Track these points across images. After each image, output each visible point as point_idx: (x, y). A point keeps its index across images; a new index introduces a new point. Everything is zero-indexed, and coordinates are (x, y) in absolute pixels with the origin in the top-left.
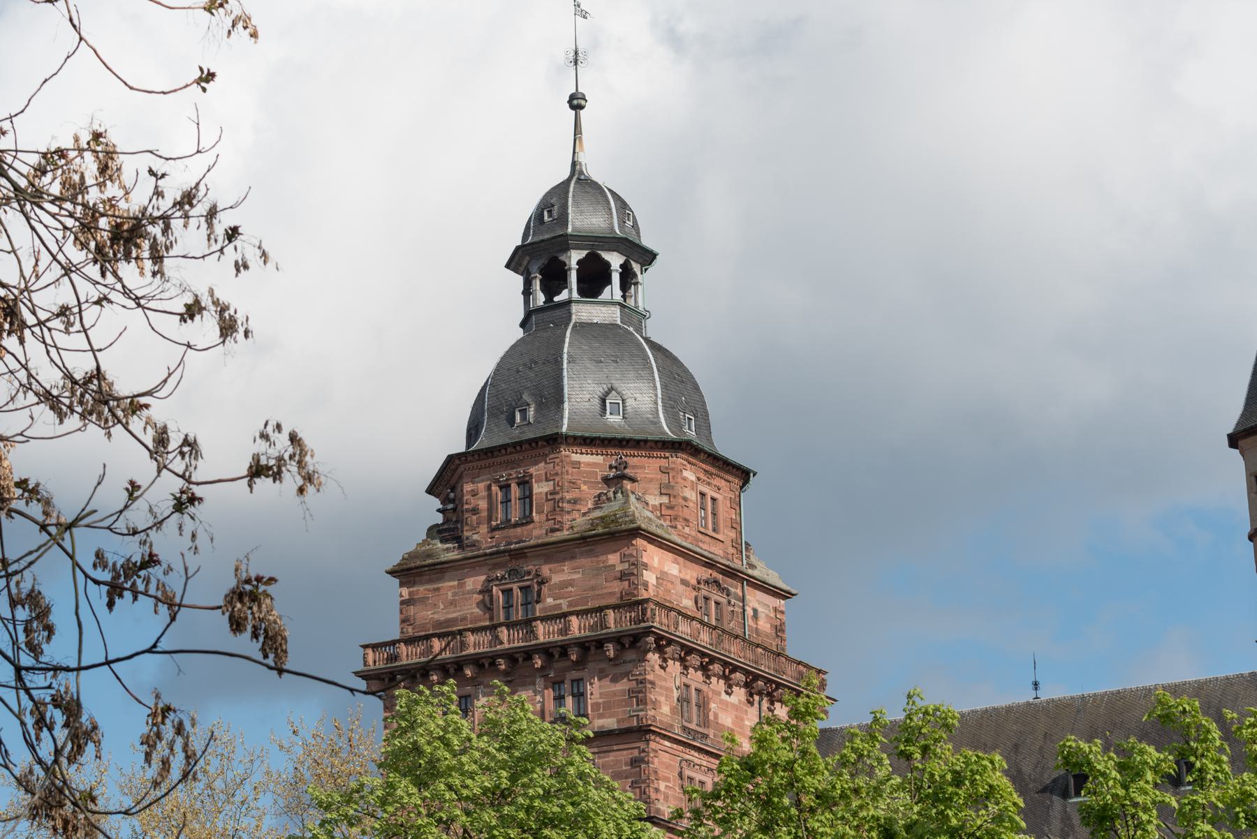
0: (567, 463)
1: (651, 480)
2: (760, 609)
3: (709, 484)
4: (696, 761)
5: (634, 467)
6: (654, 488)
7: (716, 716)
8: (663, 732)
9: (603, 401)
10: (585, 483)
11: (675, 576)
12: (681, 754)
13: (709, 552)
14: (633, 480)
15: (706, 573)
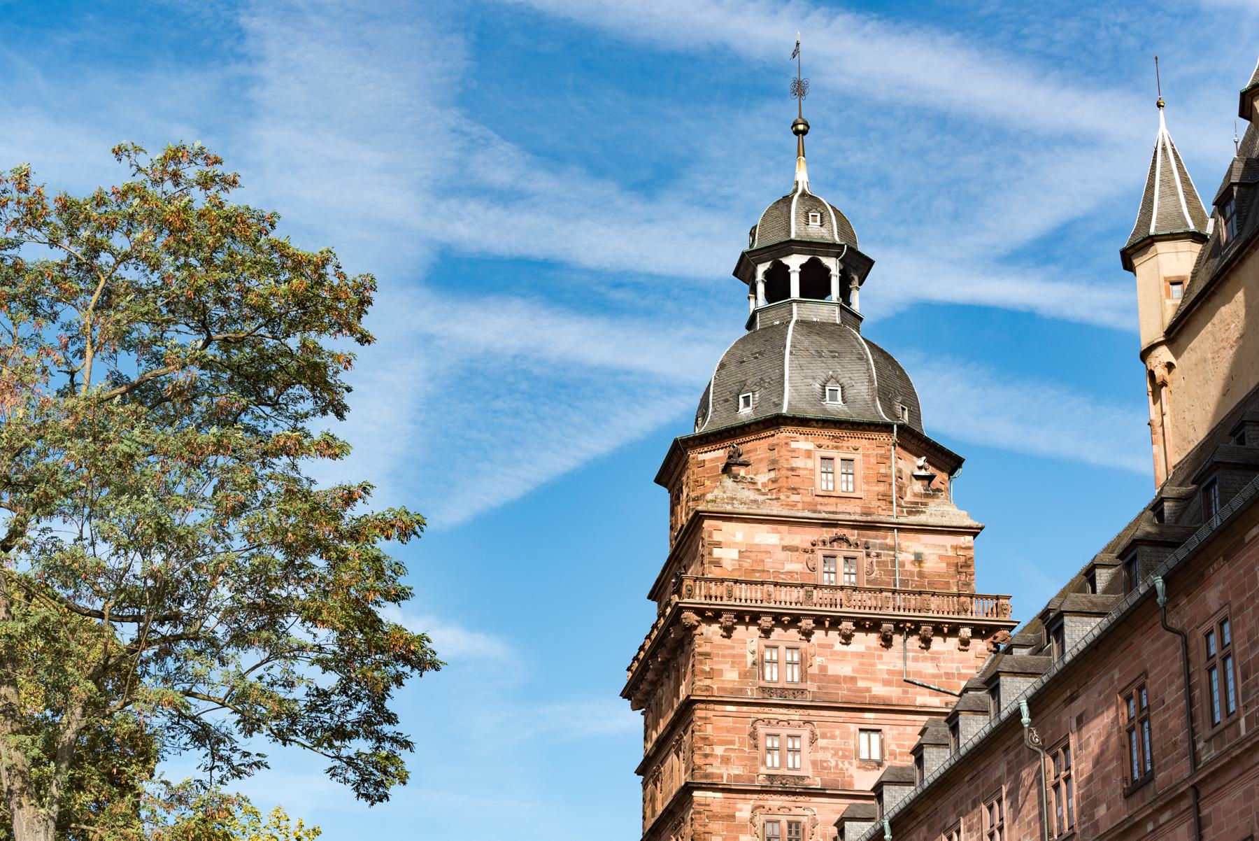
0: (694, 464)
1: (761, 460)
2: (926, 551)
3: (837, 448)
4: (780, 717)
5: (748, 452)
6: (764, 467)
7: (823, 668)
8: (709, 699)
9: (824, 387)
10: (708, 478)
11: (775, 546)
12: (752, 715)
13: (826, 512)
14: (746, 464)
15: (828, 534)
